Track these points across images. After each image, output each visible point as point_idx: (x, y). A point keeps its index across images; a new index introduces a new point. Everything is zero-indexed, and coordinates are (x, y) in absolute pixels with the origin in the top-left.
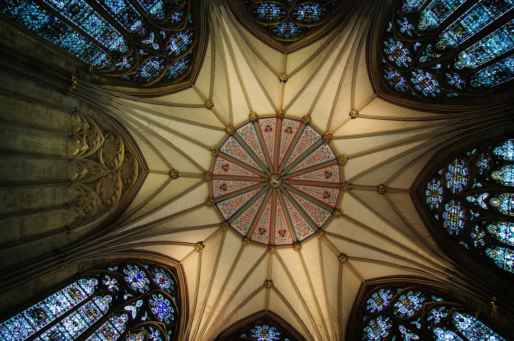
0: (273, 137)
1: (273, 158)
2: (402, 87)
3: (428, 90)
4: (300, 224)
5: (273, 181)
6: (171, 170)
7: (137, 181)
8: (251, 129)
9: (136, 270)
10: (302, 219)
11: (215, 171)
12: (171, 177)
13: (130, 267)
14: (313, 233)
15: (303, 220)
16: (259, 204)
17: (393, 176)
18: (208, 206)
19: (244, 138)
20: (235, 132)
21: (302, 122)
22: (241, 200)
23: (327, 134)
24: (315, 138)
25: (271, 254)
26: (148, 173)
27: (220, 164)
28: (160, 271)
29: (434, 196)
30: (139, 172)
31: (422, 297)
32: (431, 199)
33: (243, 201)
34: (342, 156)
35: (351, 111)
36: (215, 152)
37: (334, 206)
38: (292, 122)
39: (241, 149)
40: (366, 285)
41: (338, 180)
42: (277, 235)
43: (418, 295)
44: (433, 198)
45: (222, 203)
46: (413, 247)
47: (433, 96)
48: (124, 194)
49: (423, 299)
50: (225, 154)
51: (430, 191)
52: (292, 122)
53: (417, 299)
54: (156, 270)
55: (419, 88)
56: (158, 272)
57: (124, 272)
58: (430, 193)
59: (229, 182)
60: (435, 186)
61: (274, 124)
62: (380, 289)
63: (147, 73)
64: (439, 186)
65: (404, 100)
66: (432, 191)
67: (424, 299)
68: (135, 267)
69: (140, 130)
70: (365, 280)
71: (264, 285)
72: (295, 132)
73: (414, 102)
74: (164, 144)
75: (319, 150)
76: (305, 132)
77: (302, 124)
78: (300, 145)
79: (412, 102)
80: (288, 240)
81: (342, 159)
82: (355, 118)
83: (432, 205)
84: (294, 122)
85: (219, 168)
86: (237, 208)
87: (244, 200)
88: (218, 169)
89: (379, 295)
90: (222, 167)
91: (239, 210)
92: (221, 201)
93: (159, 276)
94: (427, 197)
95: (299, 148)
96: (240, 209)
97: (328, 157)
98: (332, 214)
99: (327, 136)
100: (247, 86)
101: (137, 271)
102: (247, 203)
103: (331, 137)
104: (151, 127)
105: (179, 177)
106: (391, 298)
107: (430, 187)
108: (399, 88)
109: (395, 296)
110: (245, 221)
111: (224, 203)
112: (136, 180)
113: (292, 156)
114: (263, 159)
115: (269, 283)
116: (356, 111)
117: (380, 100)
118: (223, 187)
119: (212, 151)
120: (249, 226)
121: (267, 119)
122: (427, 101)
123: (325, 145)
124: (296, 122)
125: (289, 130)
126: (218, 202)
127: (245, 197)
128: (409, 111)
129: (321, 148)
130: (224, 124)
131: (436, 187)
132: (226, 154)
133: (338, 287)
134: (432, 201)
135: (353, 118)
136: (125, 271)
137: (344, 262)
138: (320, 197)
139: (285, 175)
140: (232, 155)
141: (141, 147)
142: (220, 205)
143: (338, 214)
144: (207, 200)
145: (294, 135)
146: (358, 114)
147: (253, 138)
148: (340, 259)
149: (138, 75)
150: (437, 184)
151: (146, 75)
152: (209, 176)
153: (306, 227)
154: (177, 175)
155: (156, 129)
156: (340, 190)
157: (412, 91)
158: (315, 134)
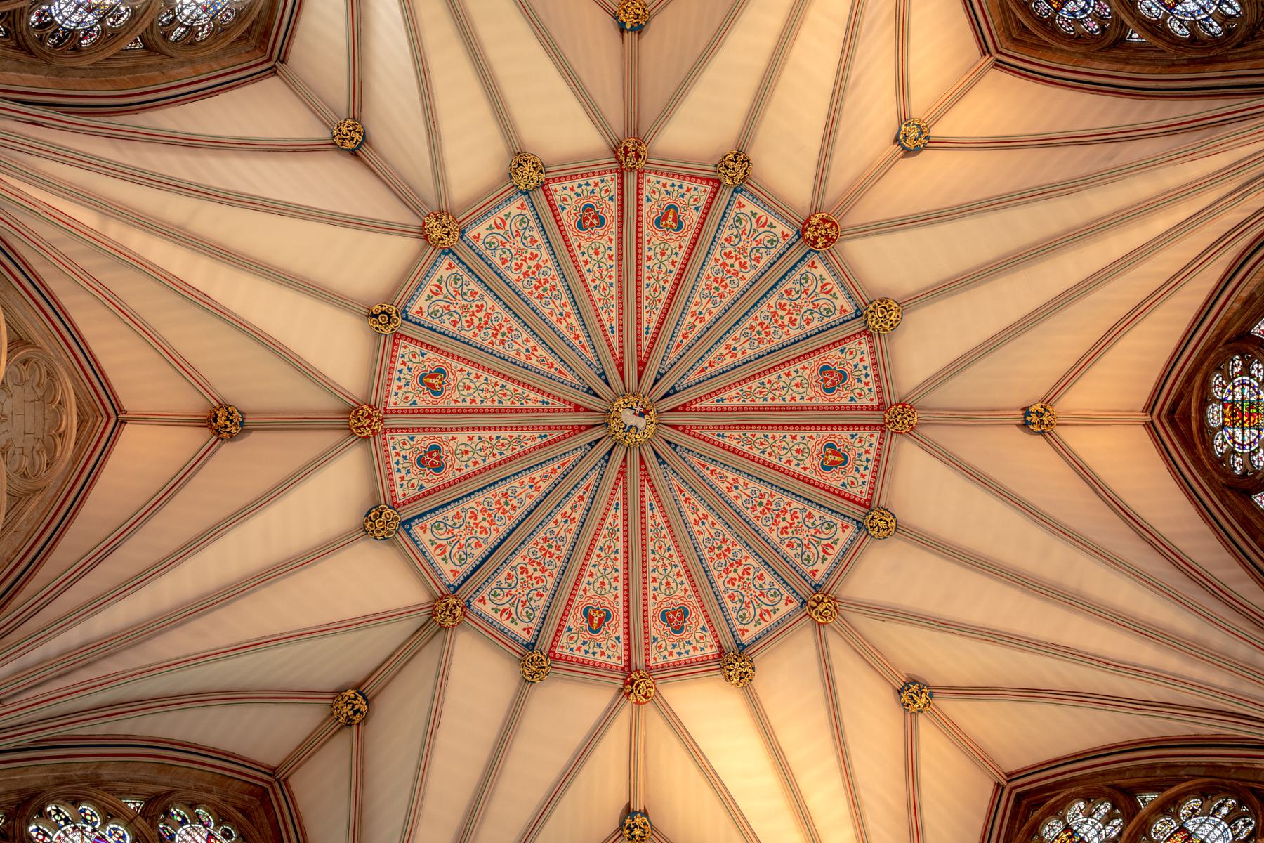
0: (610, 248)
1: (616, 334)
2: (1089, 16)
3: (1192, 14)
4: (740, 578)
5: (623, 418)
6: (216, 404)
7: (75, 461)
8: (522, 221)
9: (85, 821)
10: (746, 558)
11: (392, 399)
12: (218, 432)
13: (58, 812)
14: (791, 606)
15: (751, 561)
16: (577, 515)
17: (1078, 362)
18: (376, 538)
19: (497, 260)
20: (461, 237)
21: (716, 185)
22: (507, 503)
23: (815, 221)
24: (772, 241)
25: (637, 703)
26: (120, 423)
27: (410, 369)
28: (197, 818)
29: (1243, 422)
30: (81, 423)
31: (1243, 816)
32: (1232, 437)
33: (514, 508)
34: (882, 301)
35: (900, 129)
36: (389, 323)
37: (864, 496)
38: (677, 184)
39: (490, 304)
40: (1015, 792)
41: (874, 395)
42: (657, 629)
43: (1225, 811)
44: (1238, 433)
45: (430, 521)
46: (1185, 624)
47: (1213, 35)
48: (18, 515)
49: (1246, 825)
50: (428, 328)
51: (1225, 407)
52: (681, 187)
53: (1221, 827)
54: (178, 814)
55: (1154, 9)
56: (184, 821)
57: (34, 834)
58: (1224, 416)
59: (453, 439)
60: (1243, 384)
61: (611, 199)
62: (1067, 802)
63: (76, 9)
64: (1258, 380)
65: (1098, 67)
66: (1234, 405)
67: (1250, 823)
68: (83, 811)
69: (70, 248)
70: (1008, 775)
71: (621, 828)
72: (695, 225)
73: (1137, 68)
74: (174, 298)
75: (789, 285)
76: (731, 222)
77: (718, 189)
78: (717, 272)
79: (1129, 68)
80: (699, 646)
81: (882, 312)
82: (917, 150)
83: (1238, 459)
84: (685, 186)
85: (407, 384)
86: (493, 537)
87: (515, 502)
88: (405, 389)
89: (1067, 828)
90: (421, 382)
91: (500, 544)
92: (424, 514)
93: (189, 838)
94: (1215, 431)
95: (715, 285)
96: (503, 541)
97: (828, 311)
98: (859, 529)
99: (816, 229)
100: (495, 53)
101: (93, 824)
102: (530, 513)
103: (832, 233)
104: (115, 231)
105: (250, 431)
106: (1120, 834)
107: (1222, 392)
108: (1076, 21)
109: (1133, 823)
110: (525, 585)
111: (440, 519)
112: (69, 455)
113: (689, 319)
114: (577, 337)
115: (639, 820)
116: (919, 126)
117: (1007, 78)
118: (431, 460)
119: (377, 316)
120: (542, 602)
121: (583, 182)
122: (1187, 56)
123: (813, 265)
124: (696, 185)
125: (670, 217)
126: (412, 519)
127: (519, 491)
128: (1123, 103)
129: (798, 277)
130: (415, 211)
131: (1247, 388)
132: (431, 329)
133: (909, 811)
134: (1234, 442)
135: (909, 152)
136: (38, 829)
137: (921, 711)
138: (809, 466)
139: (667, 395)
140: (454, 330)
141: (78, 317)
142: (424, 528)
143: (882, 524)
144: (369, 512)
145: (690, 234)
146: (927, 138)
147: (534, 257)
148: (905, 698)
149: (39, 15)
150: (1252, 376)
151: (75, 18)
152: (369, 416)
153: (766, 586)
154: (242, 424)
155: (137, 241)
156: (883, 432)
157: (1128, 22)
158: (772, 226)
